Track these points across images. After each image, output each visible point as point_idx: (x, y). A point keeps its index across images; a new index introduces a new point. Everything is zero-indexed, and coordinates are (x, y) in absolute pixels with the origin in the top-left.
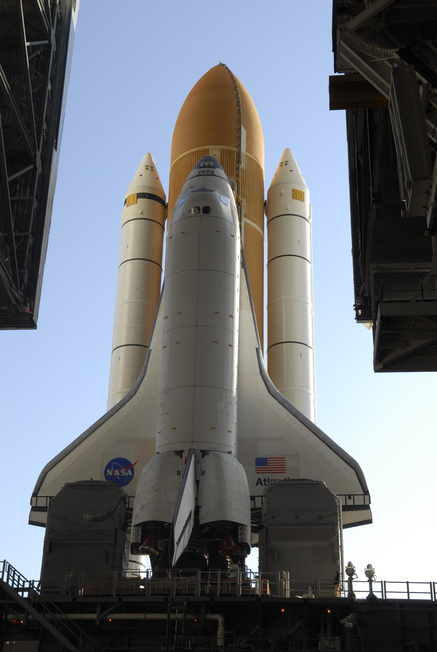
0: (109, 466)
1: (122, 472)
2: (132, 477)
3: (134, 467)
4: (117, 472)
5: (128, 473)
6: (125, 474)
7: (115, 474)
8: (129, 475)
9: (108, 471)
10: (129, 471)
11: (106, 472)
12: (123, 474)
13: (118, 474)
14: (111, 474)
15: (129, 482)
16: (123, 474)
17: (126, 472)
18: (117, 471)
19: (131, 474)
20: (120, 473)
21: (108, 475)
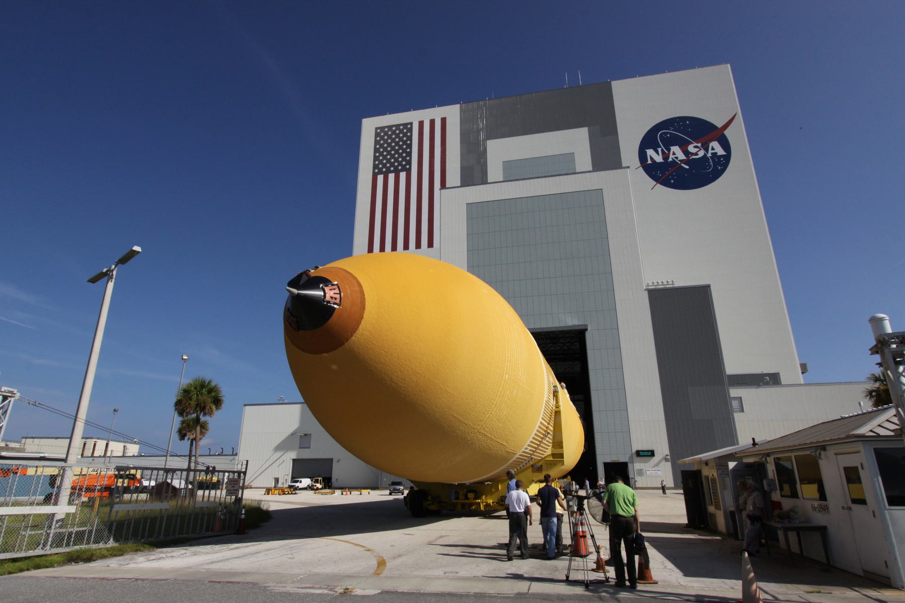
0: (649, 141)
1: (691, 148)
2: (727, 158)
3: (726, 132)
4: (677, 152)
5: (710, 151)
6: (701, 153)
8: (714, 154)
11: (642, 156)
13: (681, 156)
14: (659, 159)
16: (696, 154)
17: (707, 150)
19: (720, 151)
20: (686, 153)
21: (649, 162)
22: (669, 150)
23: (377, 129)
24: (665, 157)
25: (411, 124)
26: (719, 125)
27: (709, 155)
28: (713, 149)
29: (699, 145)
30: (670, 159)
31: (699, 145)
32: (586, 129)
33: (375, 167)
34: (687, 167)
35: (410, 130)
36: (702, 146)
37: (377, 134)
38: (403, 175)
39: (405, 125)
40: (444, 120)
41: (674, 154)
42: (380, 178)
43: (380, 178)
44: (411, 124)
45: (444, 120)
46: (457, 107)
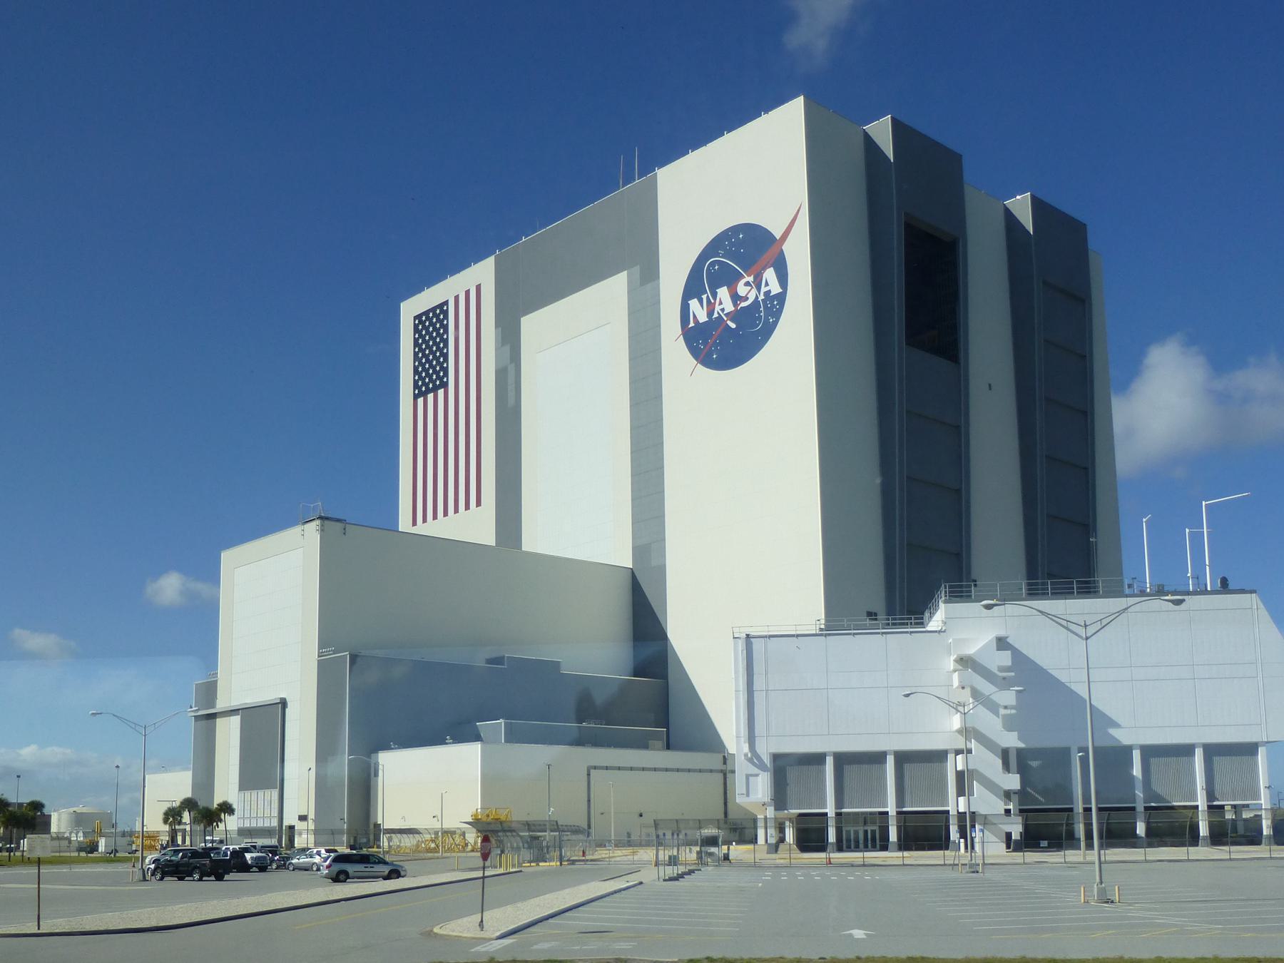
1: (742, 290)
2: (781, 298)
3: (784, 248)
5: (764, 289)
7: (718, 308)
9: (694, 303)
10: (770, 275)
12: (746, 299)
13: (729, 307)
14: (703, 317)
15: (776, 323)
17: (759, 289)
18: (723, 293)
19: (775, 288)
20: (736, 298)
21: (692, 324)
22: (715, 295)
23: (415, 318)
24: (710, 313)
25: (446, 303)
26: (778, 236)
27: (761, 297)
28: (767, 284)
29: (751, 279)
30: (716, 315)
31: (751, 279)
32: (625, 273)
33: (416, 386)
34: (733, 326)
35: (446, 313)
36: (755, 278)
37: (416, 330)
38: (441, 392)
39: (441, 306)
40: (478, 288)
41: (721, 303)
42: (420, 401)
43: (420, 401)
44: (446, 303)
45: (478, 288)
46: (491, 261)
